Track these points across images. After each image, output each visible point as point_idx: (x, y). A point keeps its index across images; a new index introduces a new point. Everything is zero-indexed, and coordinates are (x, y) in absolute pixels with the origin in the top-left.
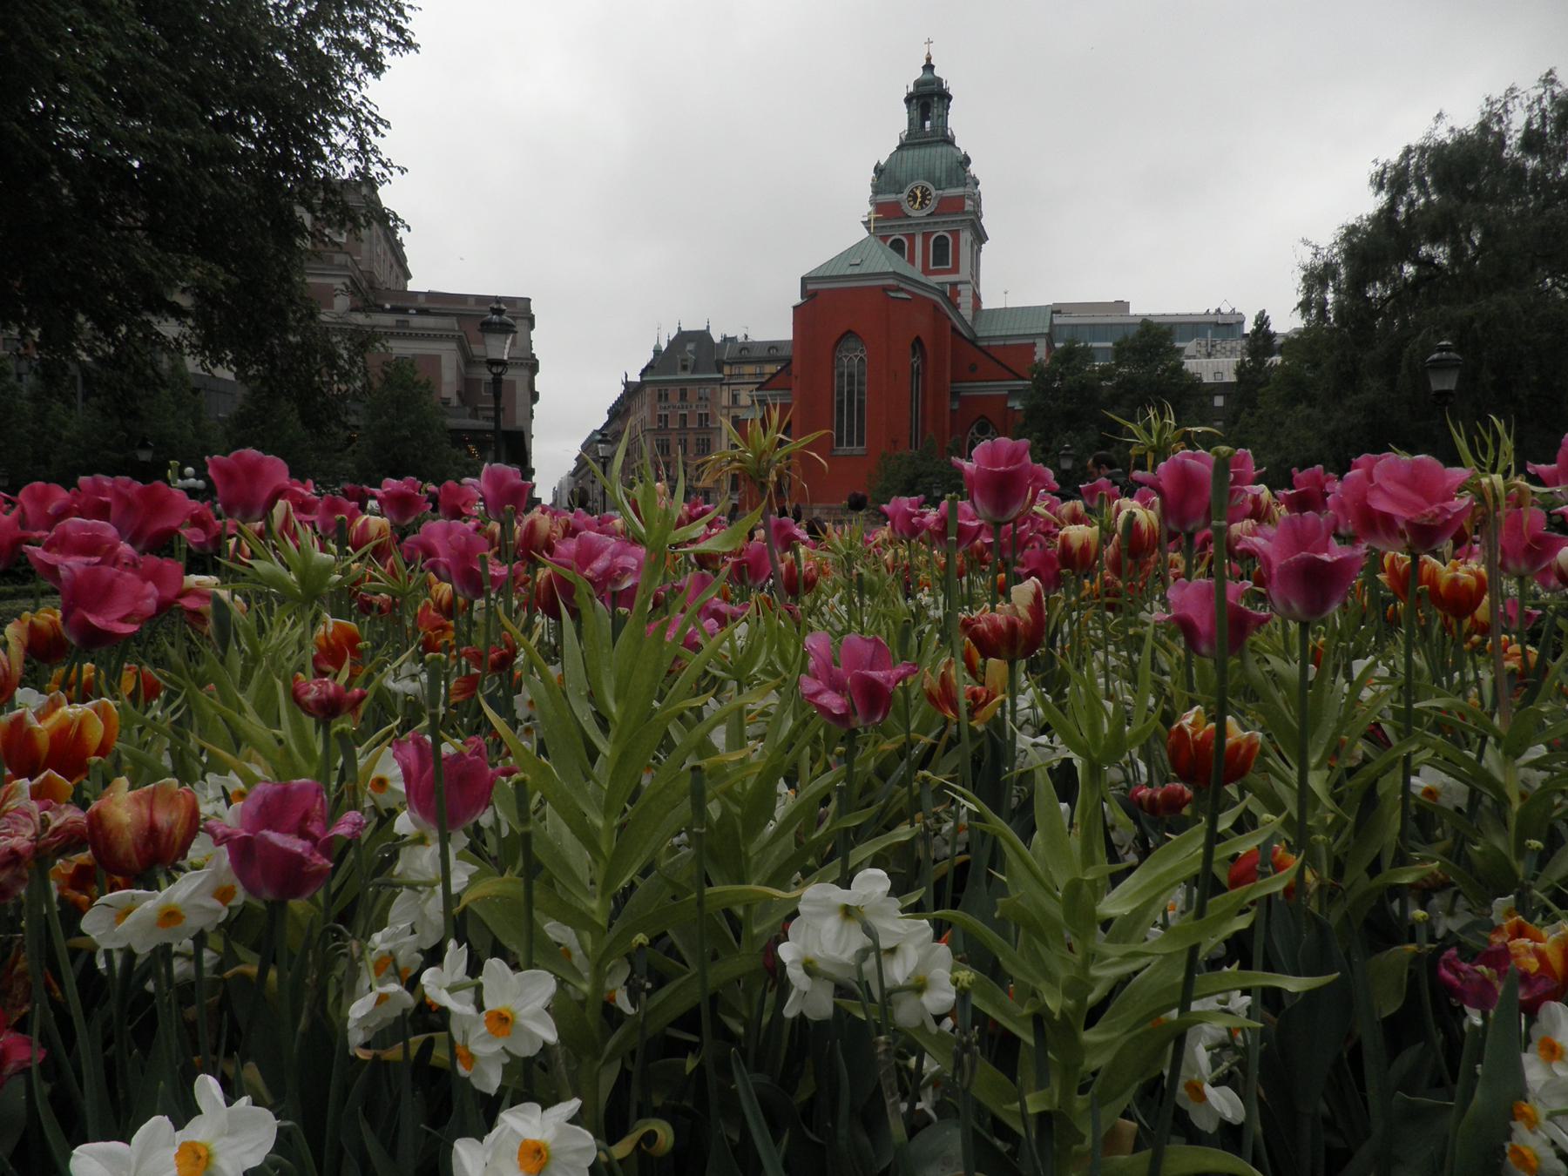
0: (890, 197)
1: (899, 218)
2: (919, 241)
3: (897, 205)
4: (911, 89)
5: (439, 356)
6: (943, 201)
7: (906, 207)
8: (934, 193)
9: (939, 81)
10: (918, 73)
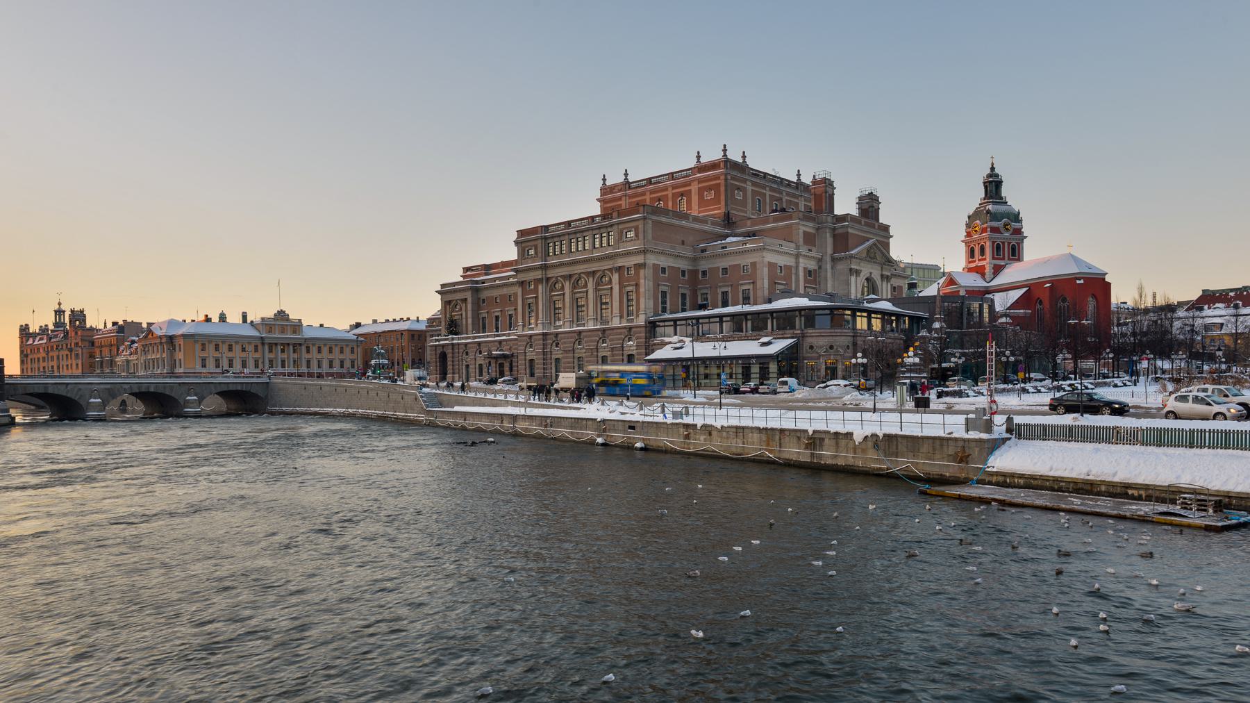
7: (1002, 230)
9: (997, 175)
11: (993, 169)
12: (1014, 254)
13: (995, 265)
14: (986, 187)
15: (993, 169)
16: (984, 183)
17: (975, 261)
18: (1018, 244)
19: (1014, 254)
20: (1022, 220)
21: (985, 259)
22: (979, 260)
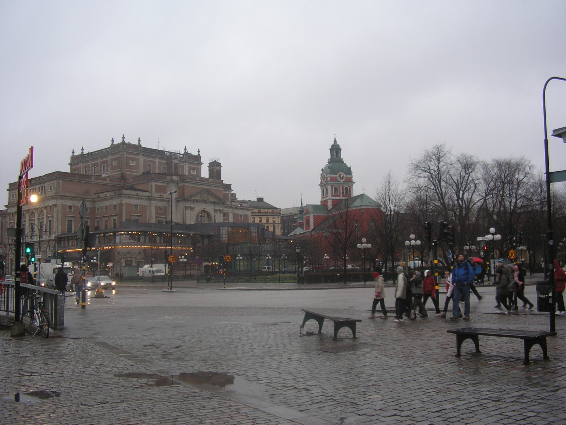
0: (334, 176)
1: (336, 181)
2: (341, 187)
3: (336, 177)
4: (331, 147)
5: (248, 215)
6: (347, 178)
7: (338, 179)
10: (333, 143)
11: (335, 141)
14: (331, 152)
15: (335, 141)
16: (330, 149)
17: (324, 198)
18: (350, 187)
21: (327, 197)
22: (326, 197)
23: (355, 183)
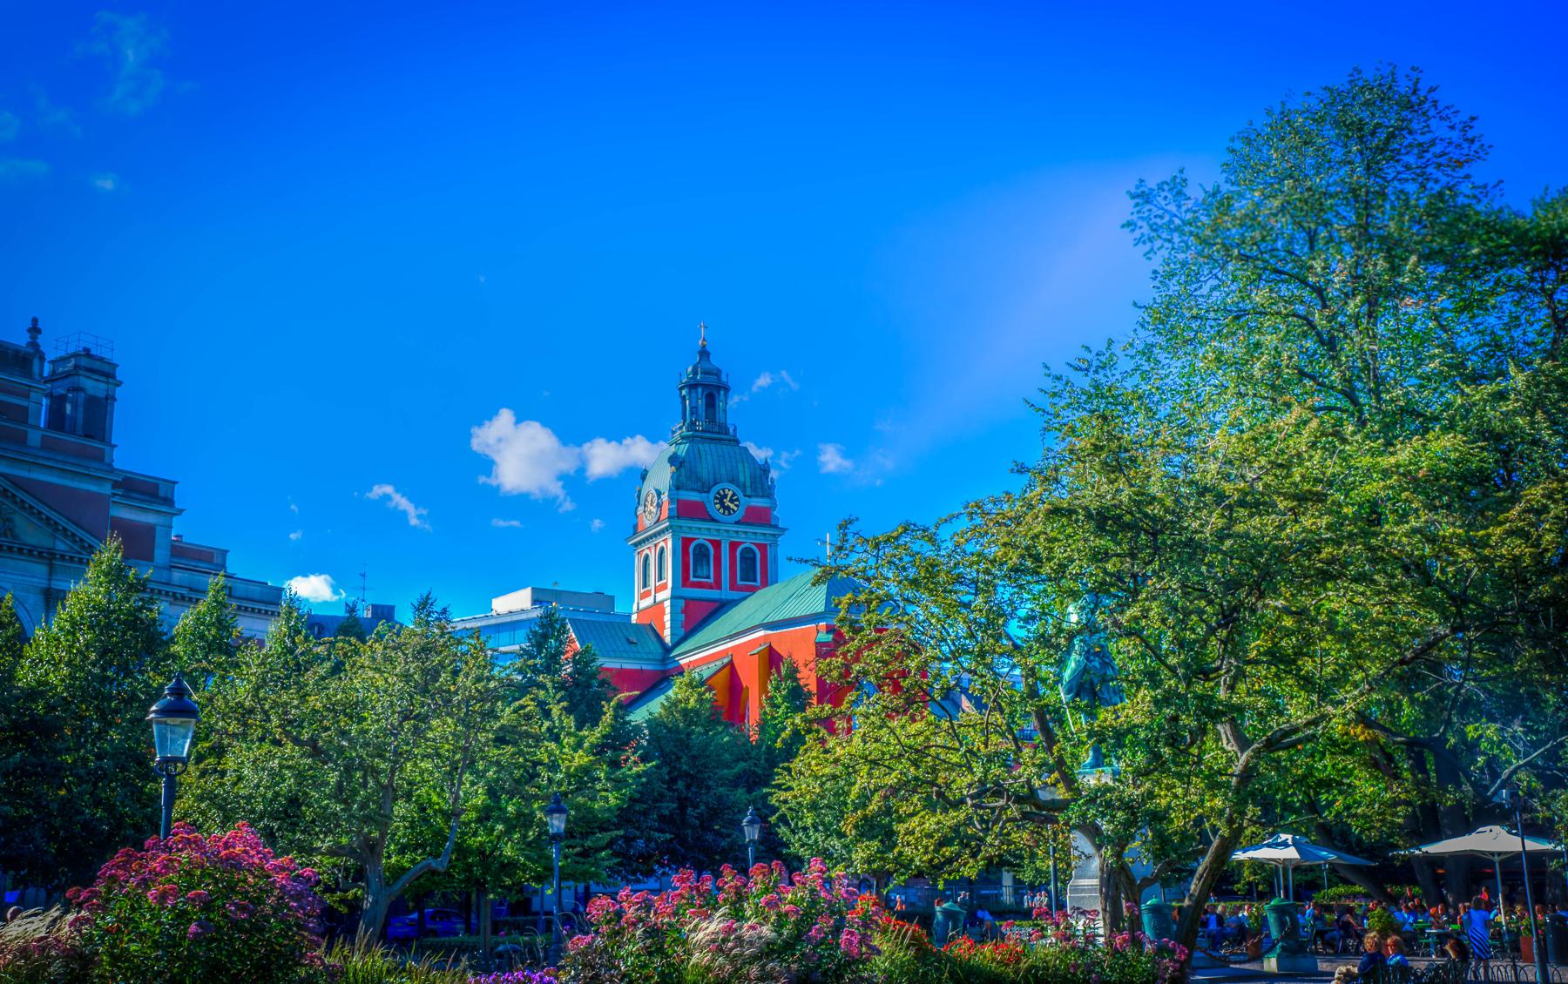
0: (694, 497)
1: (704, 520)
7: (714, 509)
8: (743, 499)
9: (718, 373)
11: (704, 353)
12: (749, 573)
13: (689, 602)
15: (704, 353)
17: (647, 595)
18: (762, 548)
19: (749, 573)
20: (771, 488)
21: (664, 587)
23: (784, 530)
